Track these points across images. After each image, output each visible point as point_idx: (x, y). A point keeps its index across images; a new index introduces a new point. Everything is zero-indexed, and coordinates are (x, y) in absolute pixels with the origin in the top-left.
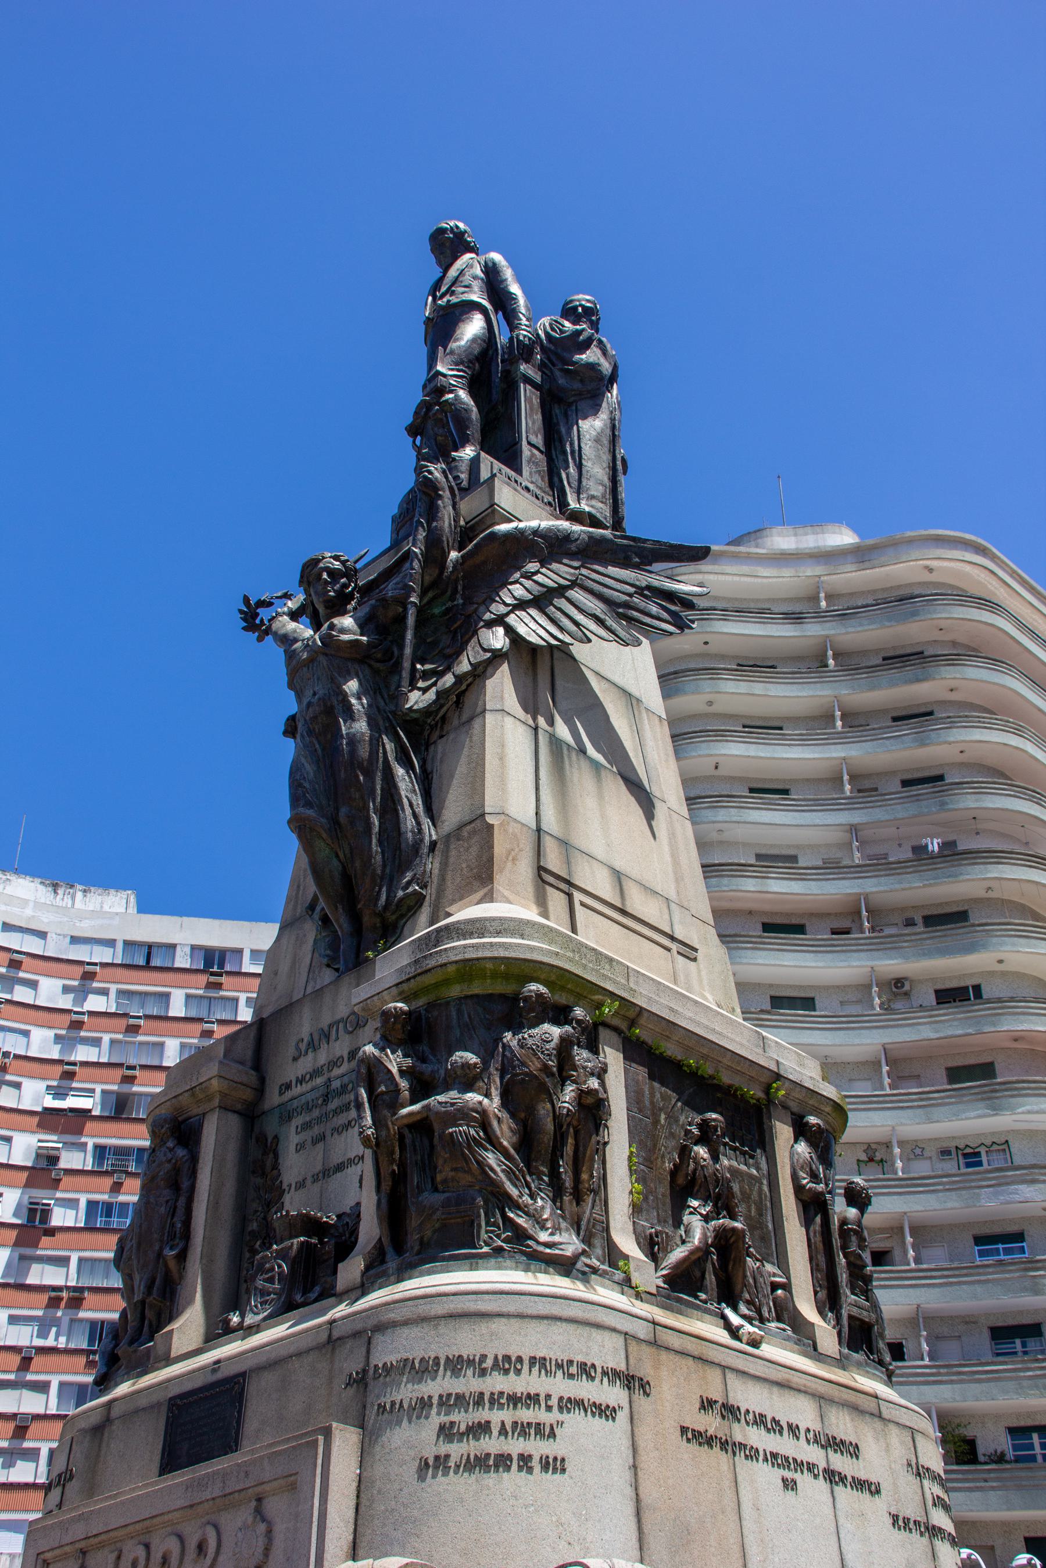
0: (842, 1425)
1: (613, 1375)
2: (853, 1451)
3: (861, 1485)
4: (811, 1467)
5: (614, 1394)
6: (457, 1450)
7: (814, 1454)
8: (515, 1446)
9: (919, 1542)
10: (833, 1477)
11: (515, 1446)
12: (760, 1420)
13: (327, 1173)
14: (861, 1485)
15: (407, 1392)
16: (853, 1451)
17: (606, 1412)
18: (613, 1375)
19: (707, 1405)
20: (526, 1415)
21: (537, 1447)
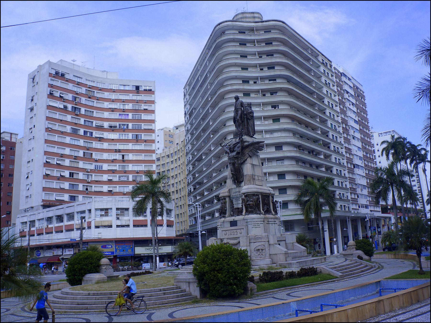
0: (275, 220)
1: (263, 221)
2: (275, 222)
3: (276, 224)
4: (273, 224)
5: (263, 222)
6: (254, 227)
7: (273, 223)
8: (258, 226)
9: (279, 226)
10: (274, 224)
11: (258, 226)
12: (270, 221)
13: (238, 204)
14: (276, 224)
15: (250, 223)
16: (275, 222)
17: (262, 224)
18: (263, 221)
19: (268, 221)
20: (258, 224)
21: (259, 226)
